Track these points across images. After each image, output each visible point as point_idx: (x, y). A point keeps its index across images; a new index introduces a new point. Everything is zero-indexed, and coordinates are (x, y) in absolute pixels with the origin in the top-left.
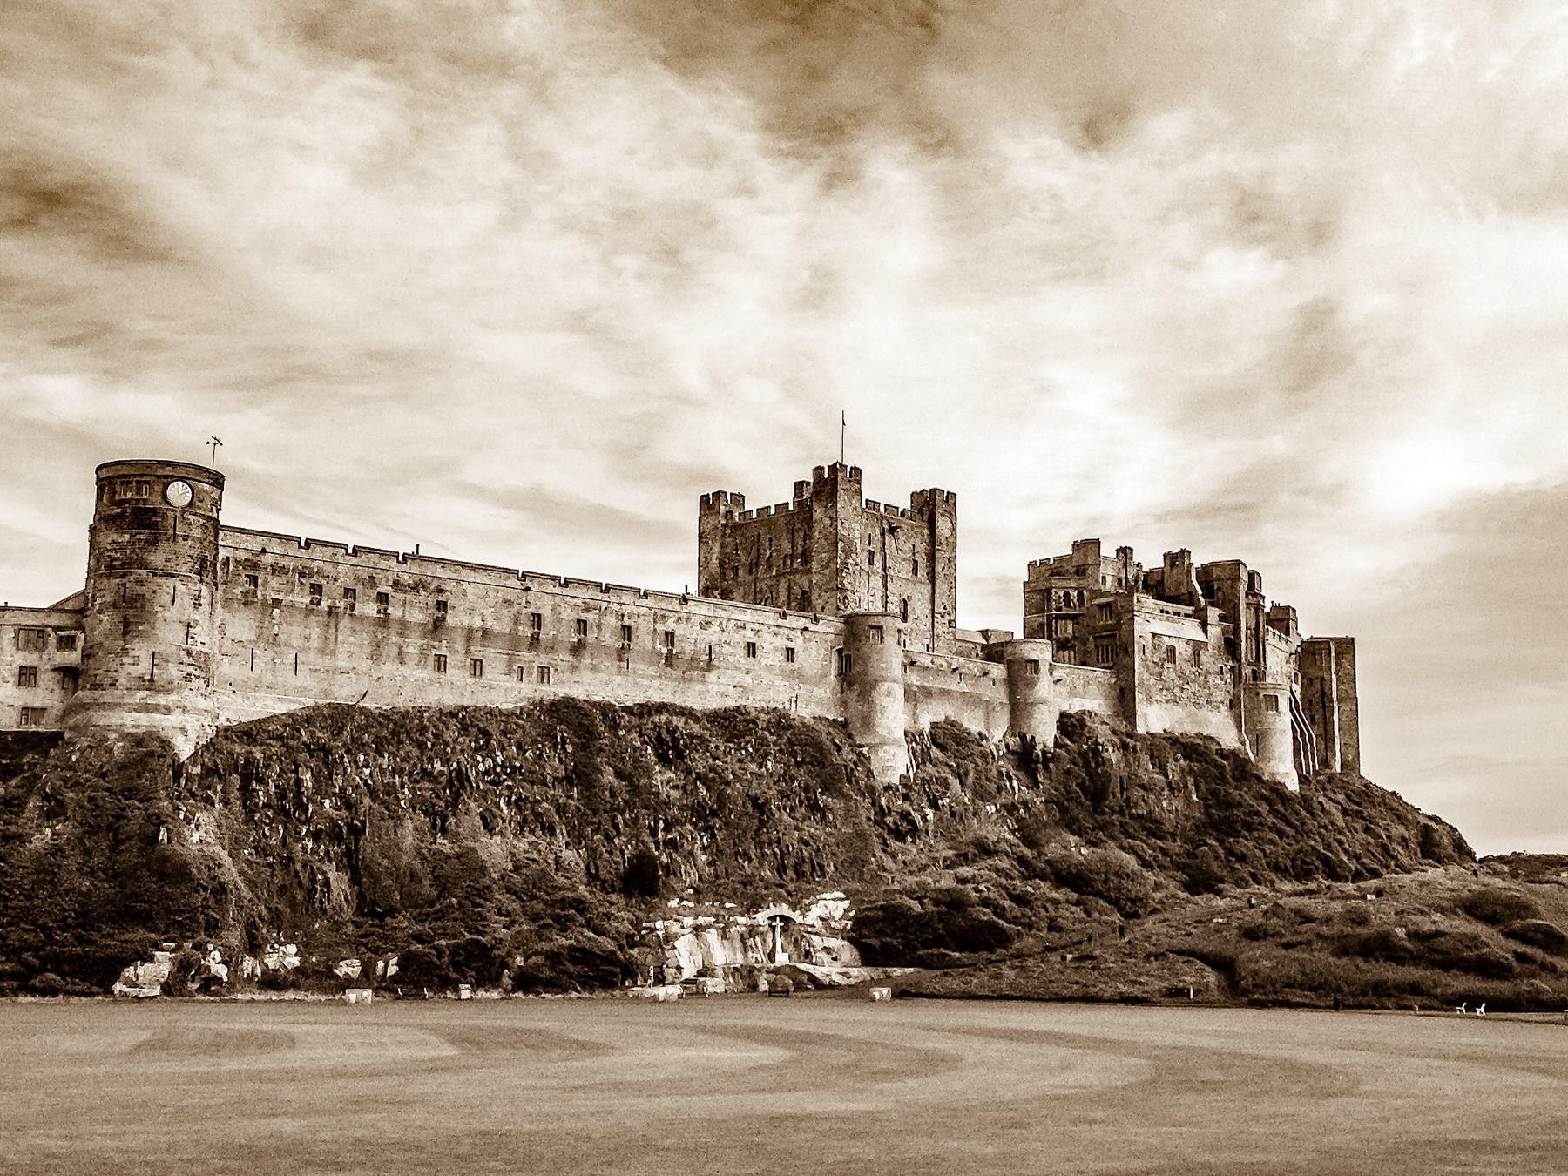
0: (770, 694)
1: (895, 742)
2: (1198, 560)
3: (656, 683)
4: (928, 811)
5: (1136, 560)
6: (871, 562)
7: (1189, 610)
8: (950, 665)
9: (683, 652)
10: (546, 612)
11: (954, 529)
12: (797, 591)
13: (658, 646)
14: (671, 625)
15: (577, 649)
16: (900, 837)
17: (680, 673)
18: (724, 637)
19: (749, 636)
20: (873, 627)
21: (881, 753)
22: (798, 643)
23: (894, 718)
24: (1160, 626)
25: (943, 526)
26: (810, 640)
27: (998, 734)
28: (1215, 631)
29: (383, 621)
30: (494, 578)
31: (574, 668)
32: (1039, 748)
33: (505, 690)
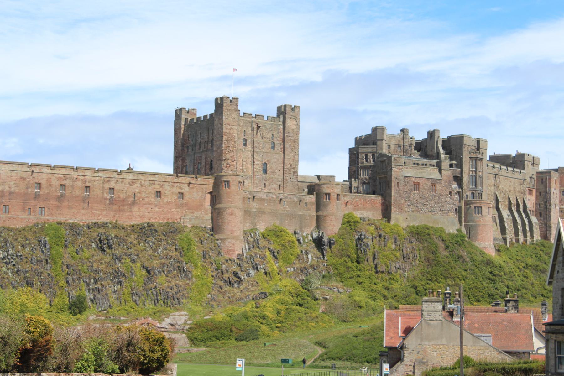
0: (169, 216)
1: (236, 238)
2: (443, 135)
3: (104, 213)
4: (251, 271)
5: (410, 135)
6: (245, 145)
7: (434, 162)
8: (278, 197)
9: (119, 197)
10: (43, 182)
11: (298, 125)
12: (209, 160)
13: (105, 195)
14: (112, 185)
16: (230, 283)
17: (118, 208)
18: (143, 189)
19: (158, 188)
20: (225, 181)
21: (227, 243)
22: (186, 189)
23: (236, 225)
24: (410, 172)
25: (290, 123)
26: (193, 188)
27: (309, 232)
28: (447, 173)
30: (15, 167)
31: (58, 208)
32: (325, 239)
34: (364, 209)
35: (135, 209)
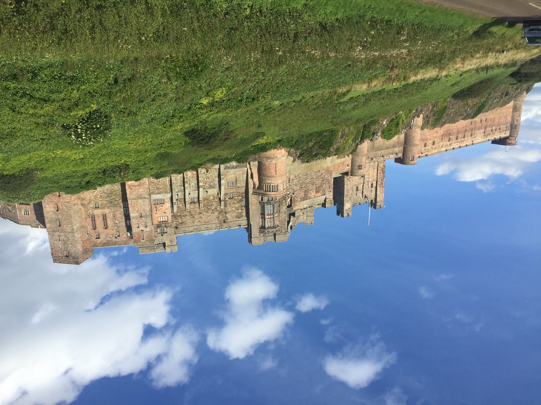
10: (470, 137)
14: (449, 143)
15: (466, 131)
29: (493, 126)
31: (466, 126)
33: (477, 119)
34: (339, 164)
35: (442, 133)
